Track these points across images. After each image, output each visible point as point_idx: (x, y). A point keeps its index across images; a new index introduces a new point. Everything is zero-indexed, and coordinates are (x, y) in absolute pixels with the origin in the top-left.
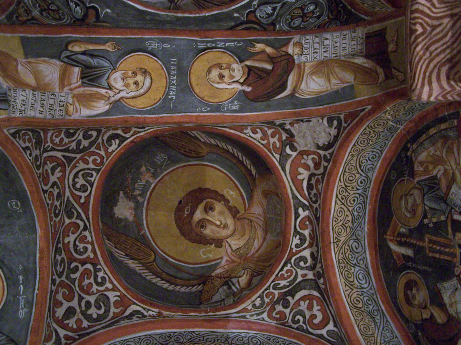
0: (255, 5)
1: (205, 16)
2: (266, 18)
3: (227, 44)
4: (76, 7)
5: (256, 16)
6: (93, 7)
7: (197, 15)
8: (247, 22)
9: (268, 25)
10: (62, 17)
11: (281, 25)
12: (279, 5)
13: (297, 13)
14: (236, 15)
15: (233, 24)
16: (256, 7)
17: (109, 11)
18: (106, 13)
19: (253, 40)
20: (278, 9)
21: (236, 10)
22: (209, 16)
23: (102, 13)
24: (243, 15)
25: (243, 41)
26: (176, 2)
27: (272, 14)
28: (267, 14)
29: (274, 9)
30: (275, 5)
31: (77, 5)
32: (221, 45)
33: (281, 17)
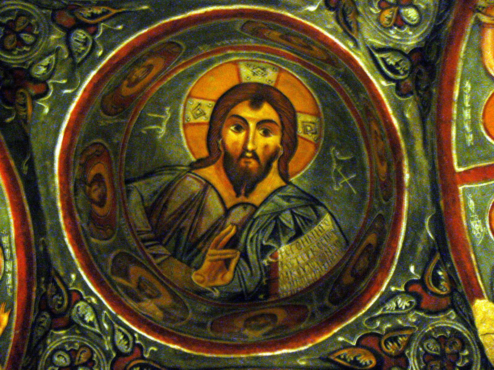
0: (90, 299)
1: (63, 237)
2: (79, 315)
3: (9, 275)
4: (45, 67)
5: (77, 302)
6: (48, 90)
7: (63, 227)
8: (69, 292)
9: (70, 317)
10: (15, 53)
11: (64, 338)
12: (97, 330)
13: (80, 357)
14: (73, 276)
15: (62, 273)
16: (89, 301)
17: (47, 110)
18: (42, 108)
19: (12, 310)
20: (93, 329)
21: (79, 276)
22: (64, 242)
23: (42, 102)
24: (74, 285)
25: (13, 296)
26: (193, 171)
27: (85, 322)
28: (84, 316)
29: (91, 324)
30: (96, 325)
31: (48, 67)
32: (9, 267)
33: (80, 335)
